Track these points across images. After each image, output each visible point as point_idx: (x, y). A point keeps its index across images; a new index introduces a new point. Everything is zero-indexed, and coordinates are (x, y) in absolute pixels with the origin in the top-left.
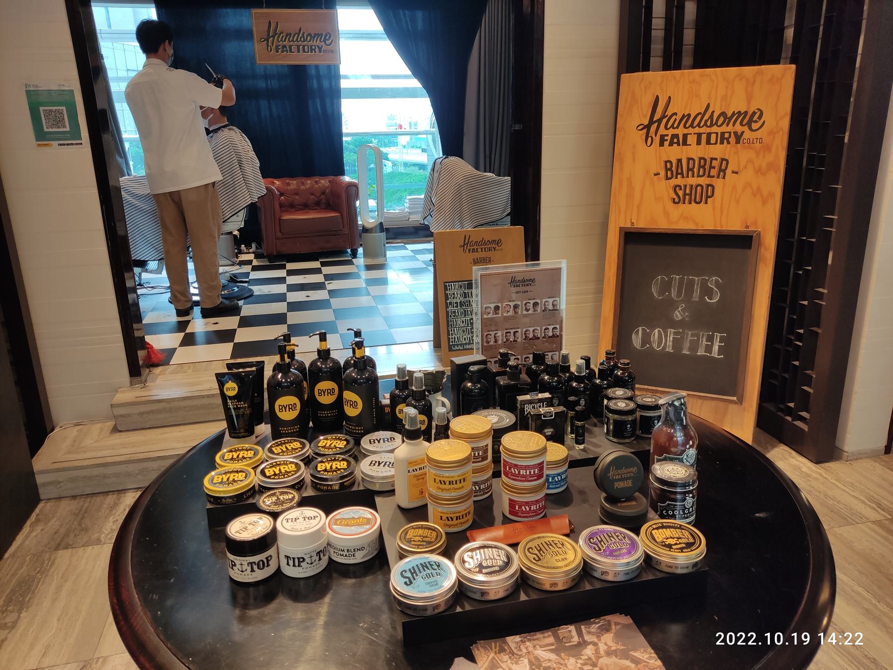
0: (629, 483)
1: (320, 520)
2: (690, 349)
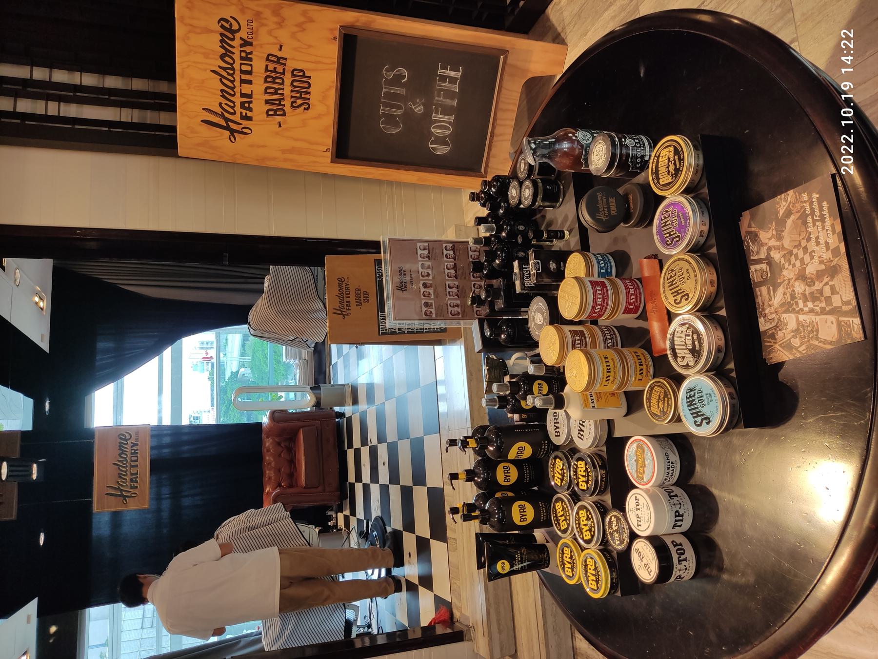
0: (612, 200)
1: (640, 494)
2: (452, 99)
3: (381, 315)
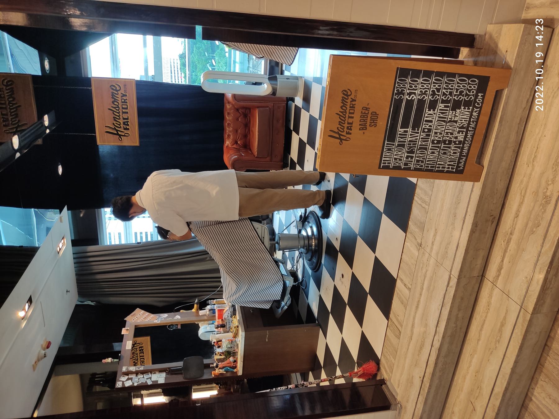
3: (387, 144)
